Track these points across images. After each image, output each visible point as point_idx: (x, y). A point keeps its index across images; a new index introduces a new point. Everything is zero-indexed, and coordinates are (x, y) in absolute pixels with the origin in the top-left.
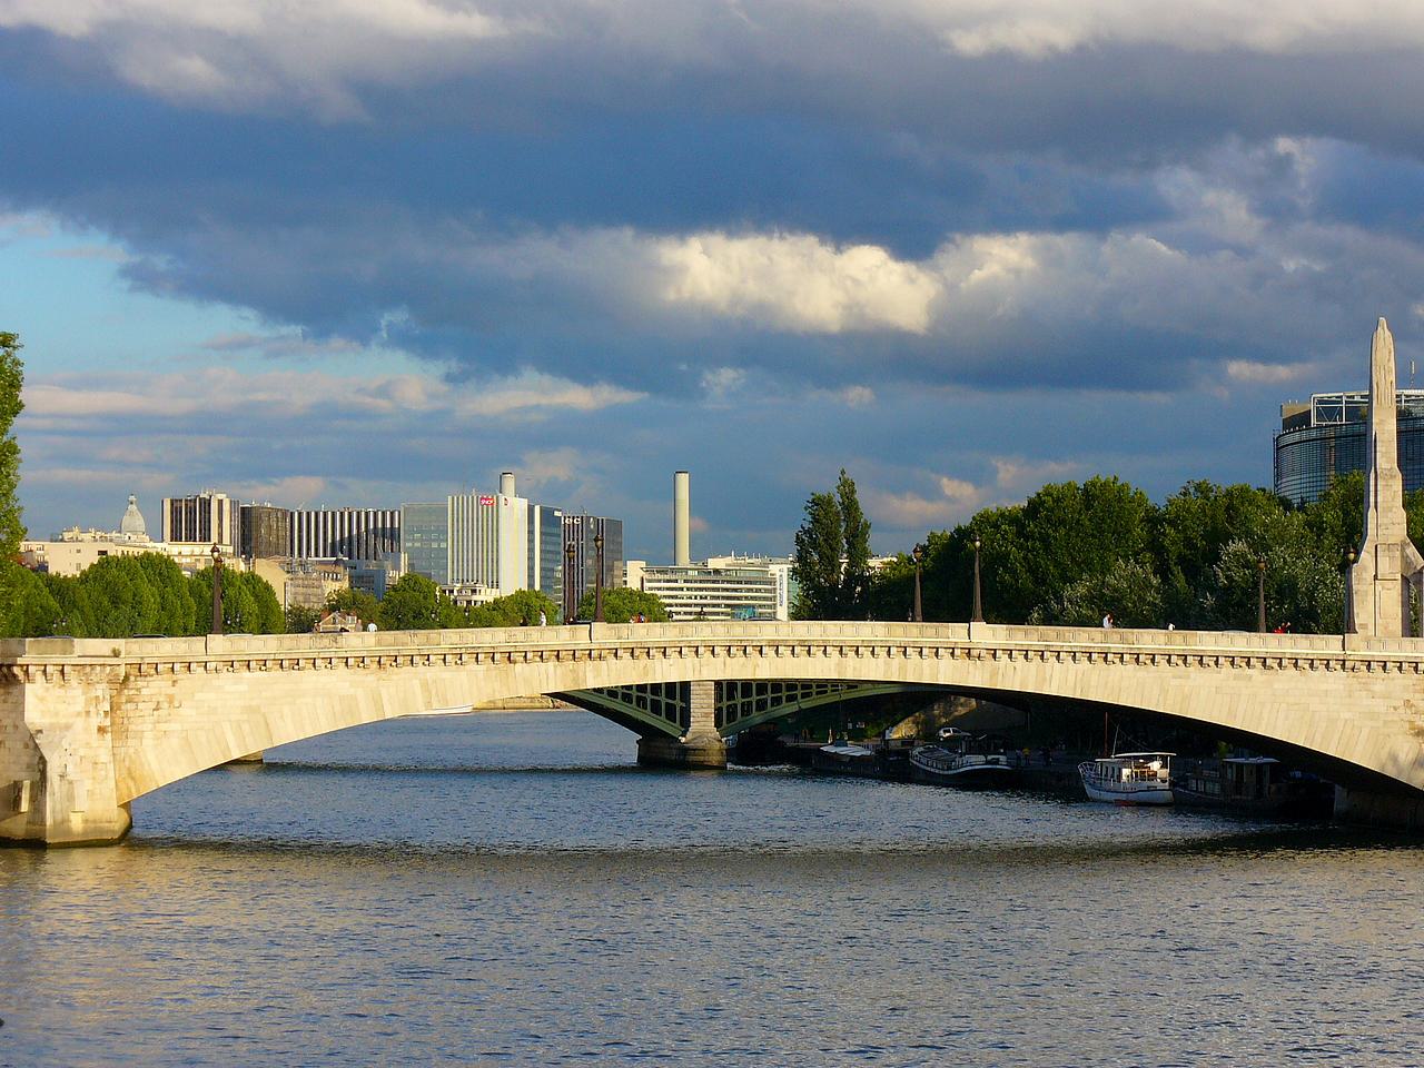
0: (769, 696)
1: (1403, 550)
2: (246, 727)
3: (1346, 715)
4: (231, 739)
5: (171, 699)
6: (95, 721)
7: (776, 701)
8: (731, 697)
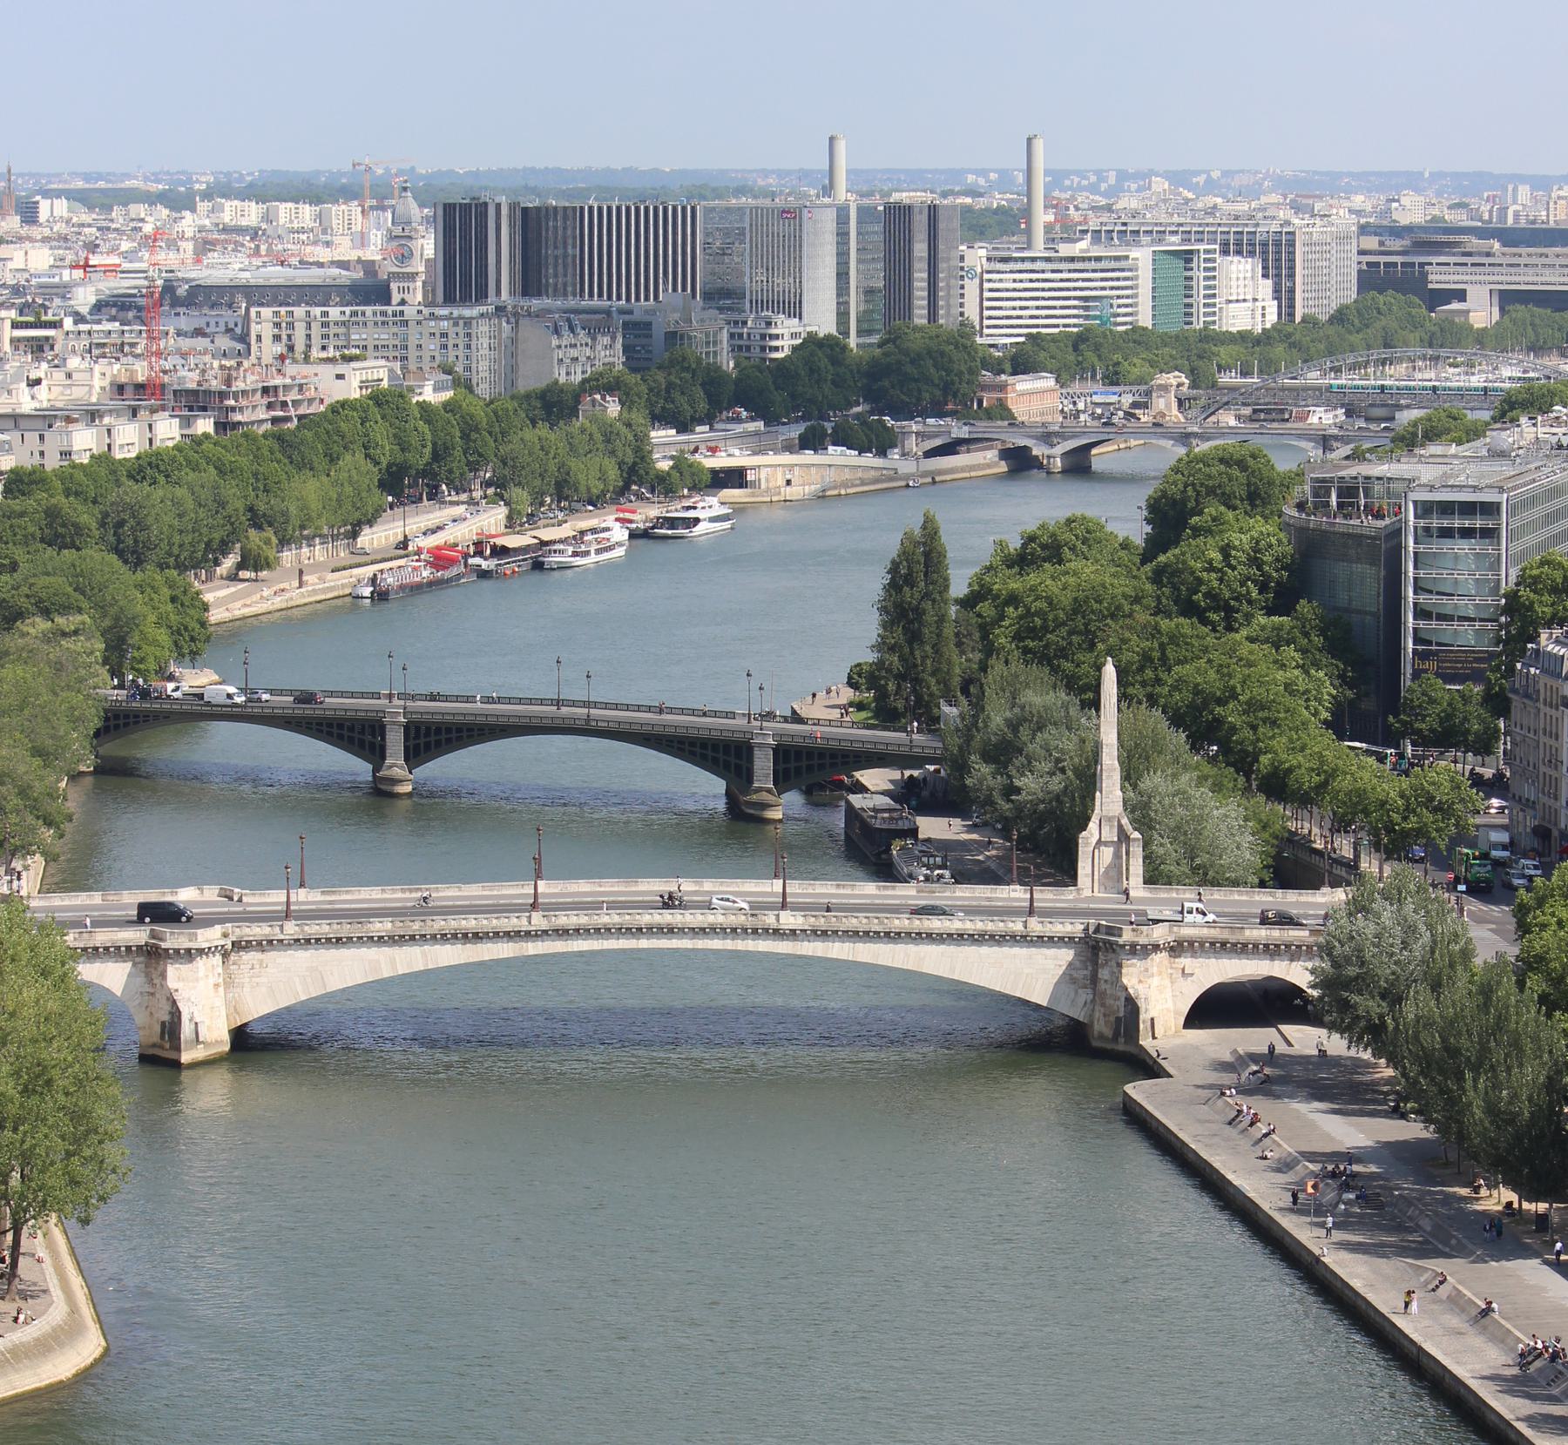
0: (816, 762)
1: (1119, 821)
2: (309, 980)
4: (299, 989)
5: (261, 962)
6: (212, 981)
7: (821, 767)
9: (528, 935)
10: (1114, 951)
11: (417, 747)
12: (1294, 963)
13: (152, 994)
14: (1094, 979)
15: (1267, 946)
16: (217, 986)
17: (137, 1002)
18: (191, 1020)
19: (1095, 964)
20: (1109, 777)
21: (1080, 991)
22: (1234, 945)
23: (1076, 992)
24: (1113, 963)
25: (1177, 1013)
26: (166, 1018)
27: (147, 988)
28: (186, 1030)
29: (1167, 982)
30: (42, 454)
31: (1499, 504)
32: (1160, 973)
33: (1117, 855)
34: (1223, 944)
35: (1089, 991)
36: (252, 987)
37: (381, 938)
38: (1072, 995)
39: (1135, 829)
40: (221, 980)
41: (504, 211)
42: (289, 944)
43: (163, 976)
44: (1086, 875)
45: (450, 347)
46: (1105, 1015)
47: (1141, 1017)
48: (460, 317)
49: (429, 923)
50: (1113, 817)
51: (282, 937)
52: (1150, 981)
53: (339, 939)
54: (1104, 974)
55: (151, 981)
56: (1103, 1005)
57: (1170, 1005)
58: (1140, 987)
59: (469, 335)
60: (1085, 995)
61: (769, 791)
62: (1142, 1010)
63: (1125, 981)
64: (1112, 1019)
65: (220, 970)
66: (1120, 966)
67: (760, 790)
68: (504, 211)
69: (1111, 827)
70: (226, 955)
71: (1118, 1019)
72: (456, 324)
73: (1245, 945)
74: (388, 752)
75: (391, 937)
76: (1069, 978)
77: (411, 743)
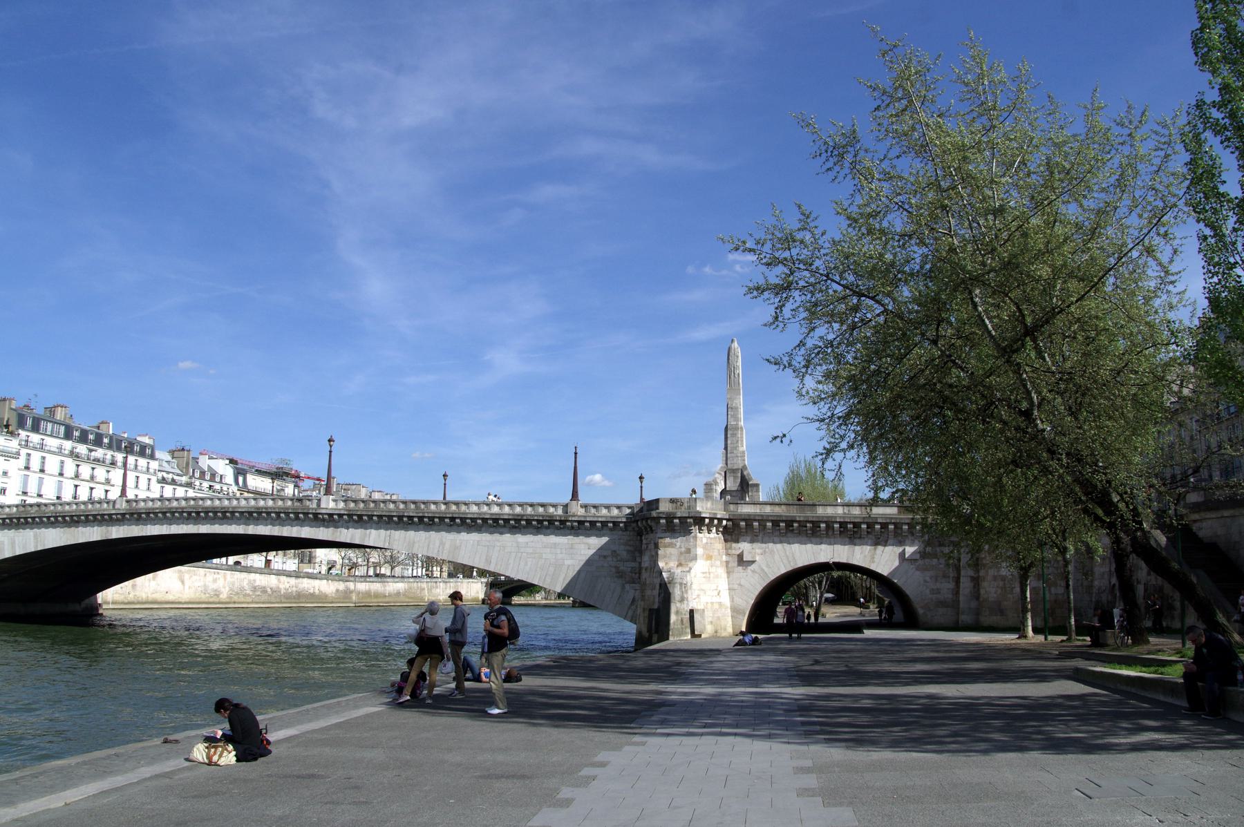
3: (568, 562)
12: (880, 548)
21: (627, 586)
22: (802, 524)
23: (623, 588)
25: (735, 611)
32: (709, 557)
34: (789, 523)
50: (737, 469)
54: (646, 560)
57: (726, 599)
63: (661, 564)
66: (657, 547)
69: (735, 477)
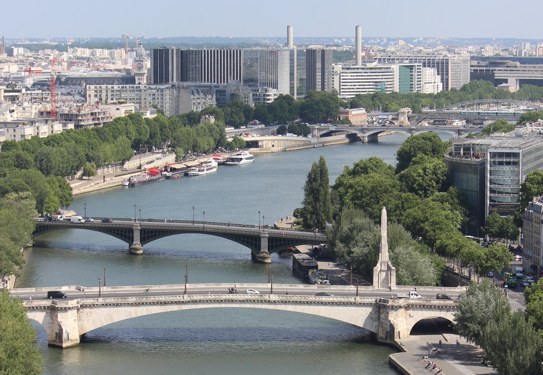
0: (282, 243)
1: (387, 263)
2: (107, 318)
4: (104, 321)
6: (73, 319)
7: (284, 244)
8: (272, 242)
9: (183, 303)
10: (386, 308)
11: (144, 237)
12: (448, 313)
13: (53, 323)
14: (379, 318)
15: (439, 306)
16: (75, 320)
17: (47, 326)
18: (66, 332)
19: (379, 313)
20: (384, 248)
21: (374, 322)
22: (427, 306)
23: (373, 323)
24: (386, 312)
25: (408, 330)
26: (58, 331)
27: (51, 321)
28: (65, 336)
29: (404, 319)
30: (15, 136)
31: (519, 153)
32: (402, 316)
33: (387, 275)
34: (424, 306)
35: (377, 322)
36: (87, 321)
37: (132, 304)
38: (371, 323)
39: (393, 266)
40: (77, 318)
41: (175, 52)
42: (100, 306)
43: (57, 317)
44: (376, 282)
45: (156, 99)
46: (383, 330)
47: (395, 331)
48: (159, 89)
49: (149, 298)
50: (386, 262)
51: (98, 303)
52: (398, 318)
53: (117, 304)
54: (382, 316)
55: (52, 319)
56: (382, 327)
57: (405, 327)
58: (395, 321)
59: (162, 95)
60: (376, 324)
61: (266, 253)
62: (396, 329)
63: (390, 318)
64: (385, 332)
65: (76, 315)
66: (388, 313)
67: (263, 252)
68: (175, 52)
69: (385, 265)
70: (78, 310)
71: (387, 332)
72: (158, 91)
73: (431, 306)
74: (134, 239)
75: (135, 303)
76: (370, 317)
77: (142, 236)
